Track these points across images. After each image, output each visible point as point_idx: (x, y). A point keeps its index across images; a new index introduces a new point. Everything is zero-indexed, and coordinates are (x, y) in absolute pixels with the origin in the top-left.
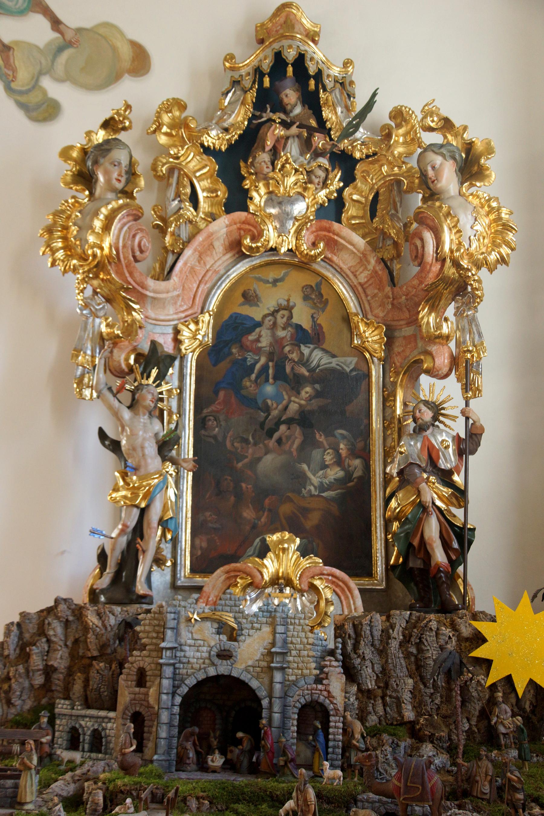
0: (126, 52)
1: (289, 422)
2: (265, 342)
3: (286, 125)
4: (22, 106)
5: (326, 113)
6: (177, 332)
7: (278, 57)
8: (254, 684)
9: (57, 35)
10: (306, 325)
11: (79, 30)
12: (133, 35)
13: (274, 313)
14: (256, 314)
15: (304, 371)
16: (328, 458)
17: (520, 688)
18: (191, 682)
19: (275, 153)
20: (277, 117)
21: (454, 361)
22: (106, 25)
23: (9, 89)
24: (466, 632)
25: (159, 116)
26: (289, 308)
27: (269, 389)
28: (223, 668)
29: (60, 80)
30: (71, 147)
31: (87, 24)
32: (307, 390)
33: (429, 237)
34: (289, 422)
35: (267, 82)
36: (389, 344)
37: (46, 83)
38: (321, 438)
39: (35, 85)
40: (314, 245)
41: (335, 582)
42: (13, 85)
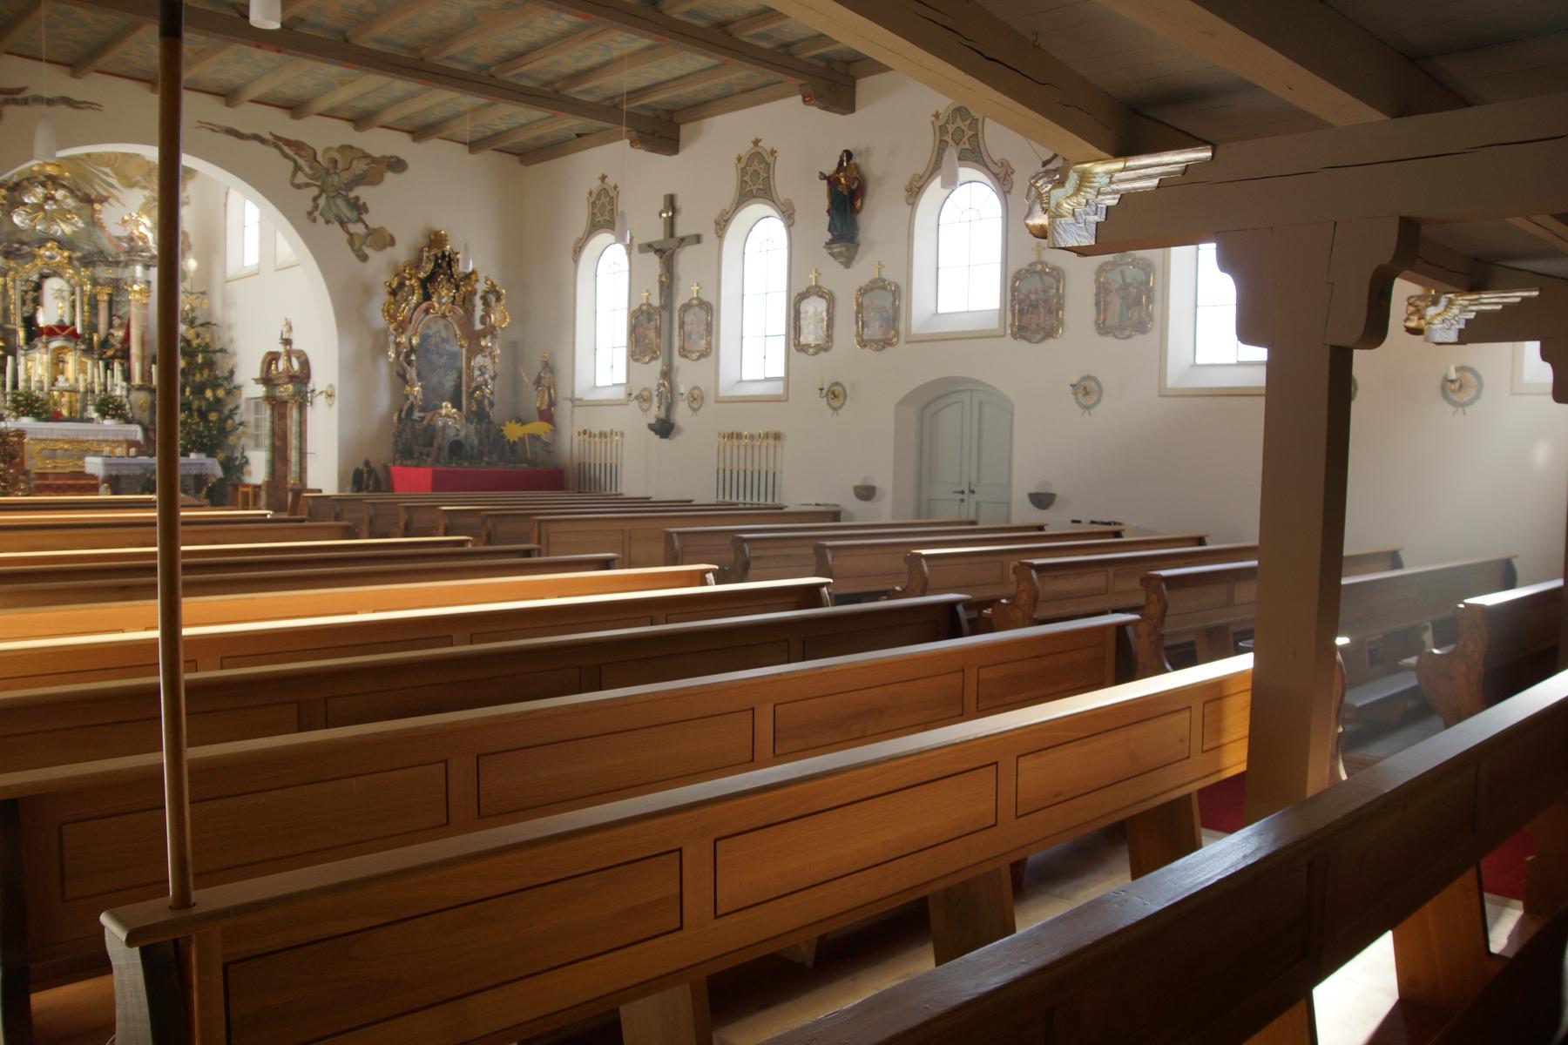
0: (387, 236)
1: (441, 368)
2: (433, 341)
3: (444, 275)
4: (358, 256)
5: (453, 269)
6: (410, 340)
7: (443, 253)
8: (464, 441)
9: (366, 231)
10: (445, 336)
11: (374, 229)
12: (391, 230)
13: (435, 333)
14: (431, 332)
15: (443, 351)
16: (451, 378)
17: (511, 441)
18: (451, 440)
19: (439, 284)
20: (441, 271)
21: (490, 354)
22: (382, 228)
23: (354, 250)
24: (497, 428)
25: (405, 267)
26: (439, 331)
27: (435, 357)
28: (455, 438)
29: (369, 247)
30: (386, 282)
31: (376, 227)
32: (445, 358)
33: (488, 320)
34: (441, 368)
35: (440, 261)
36: (469, 346)
37: (364, 248)
38: (449, 372)
39: (360, 249)
40: (449, 313)
41: (460, 416)
42: (355, 248)
